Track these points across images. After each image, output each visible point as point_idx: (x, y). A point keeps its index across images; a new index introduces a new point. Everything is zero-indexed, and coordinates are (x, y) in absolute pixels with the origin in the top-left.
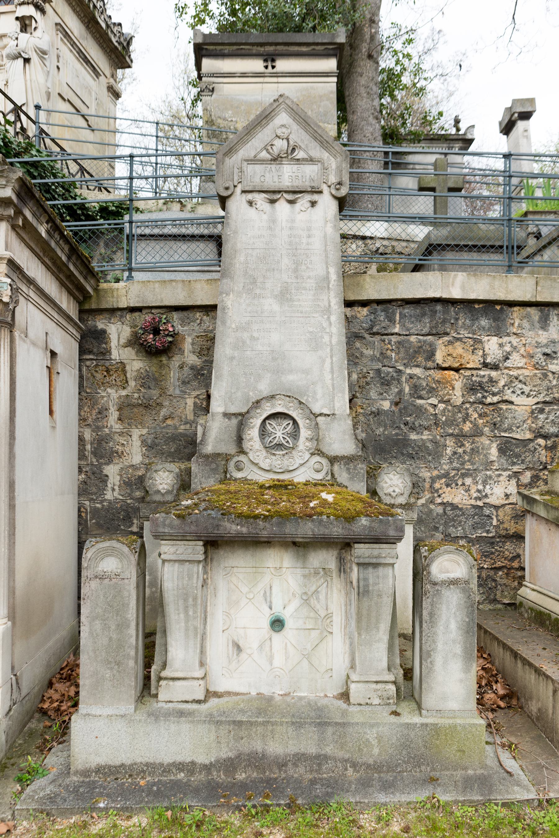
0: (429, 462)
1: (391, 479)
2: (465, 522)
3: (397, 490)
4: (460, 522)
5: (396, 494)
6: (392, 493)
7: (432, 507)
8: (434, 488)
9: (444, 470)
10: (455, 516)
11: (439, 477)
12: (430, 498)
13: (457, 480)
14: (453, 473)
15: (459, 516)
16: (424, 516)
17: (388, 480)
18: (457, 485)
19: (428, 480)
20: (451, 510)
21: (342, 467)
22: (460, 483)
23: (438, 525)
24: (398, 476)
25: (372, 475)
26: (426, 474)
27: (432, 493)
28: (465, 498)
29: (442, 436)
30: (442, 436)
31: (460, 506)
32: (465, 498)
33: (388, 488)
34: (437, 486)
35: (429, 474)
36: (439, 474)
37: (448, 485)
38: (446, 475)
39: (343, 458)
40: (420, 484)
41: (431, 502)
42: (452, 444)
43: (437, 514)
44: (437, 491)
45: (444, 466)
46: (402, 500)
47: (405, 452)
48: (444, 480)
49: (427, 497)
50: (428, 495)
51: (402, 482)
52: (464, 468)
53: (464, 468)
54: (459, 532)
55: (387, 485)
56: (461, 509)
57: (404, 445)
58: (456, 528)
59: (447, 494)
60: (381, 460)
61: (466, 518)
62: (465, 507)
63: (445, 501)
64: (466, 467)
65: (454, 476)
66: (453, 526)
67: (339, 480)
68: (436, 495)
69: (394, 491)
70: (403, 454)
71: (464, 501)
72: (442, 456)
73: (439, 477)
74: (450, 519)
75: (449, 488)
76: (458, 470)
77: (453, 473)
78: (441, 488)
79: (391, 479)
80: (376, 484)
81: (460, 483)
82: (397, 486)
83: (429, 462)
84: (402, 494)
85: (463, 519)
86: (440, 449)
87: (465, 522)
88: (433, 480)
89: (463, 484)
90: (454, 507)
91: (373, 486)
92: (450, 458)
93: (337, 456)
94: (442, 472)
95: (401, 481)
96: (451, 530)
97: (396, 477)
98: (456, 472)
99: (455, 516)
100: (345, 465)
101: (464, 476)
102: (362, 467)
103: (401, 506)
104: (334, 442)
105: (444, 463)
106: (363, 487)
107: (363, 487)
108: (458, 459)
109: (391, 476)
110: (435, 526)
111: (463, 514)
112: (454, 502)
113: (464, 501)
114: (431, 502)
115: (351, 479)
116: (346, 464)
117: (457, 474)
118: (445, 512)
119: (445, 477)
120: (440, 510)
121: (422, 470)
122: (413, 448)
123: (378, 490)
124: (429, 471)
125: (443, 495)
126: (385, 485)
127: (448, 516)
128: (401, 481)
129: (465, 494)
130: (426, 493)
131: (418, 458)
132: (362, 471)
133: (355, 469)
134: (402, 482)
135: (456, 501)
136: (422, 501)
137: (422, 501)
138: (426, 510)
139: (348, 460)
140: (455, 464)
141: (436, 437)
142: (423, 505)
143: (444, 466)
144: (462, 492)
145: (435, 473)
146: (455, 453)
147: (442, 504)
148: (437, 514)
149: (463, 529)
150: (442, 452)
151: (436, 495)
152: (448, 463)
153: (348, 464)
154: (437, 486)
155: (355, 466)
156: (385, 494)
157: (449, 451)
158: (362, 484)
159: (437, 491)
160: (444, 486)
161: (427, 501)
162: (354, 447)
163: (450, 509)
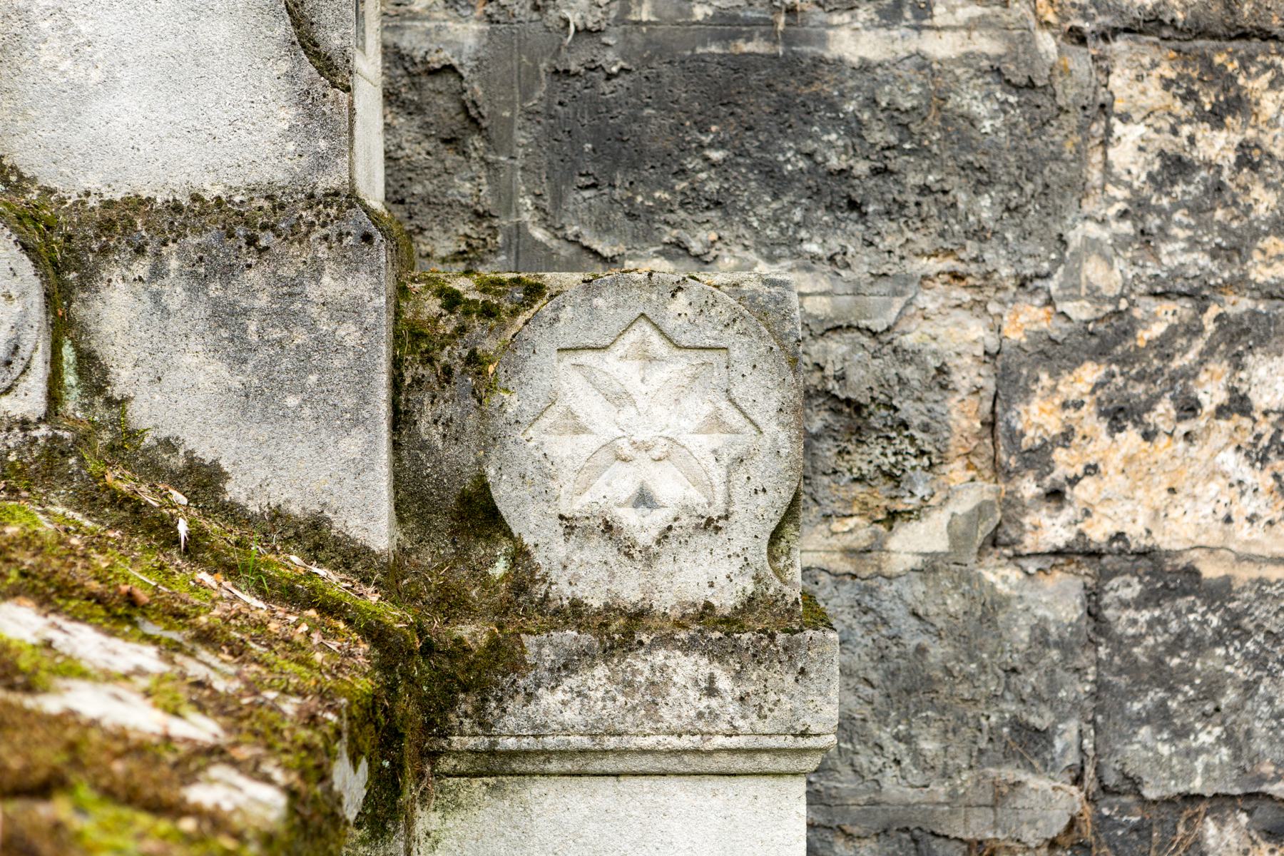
0: (979, 234)
1: (619, 398)
2: (1249, 688)
3: (673, 489)
4: (1212, 689)
5: (658, 519)
6: (629, 518)
7: (1000, 576)
8: (1014, 436)
9: (1094, 294)
10: (1175, 646)
11: (1054, 354)
12: (980, 511)
13: (1189, 374)
14: (1159, 319)
15: (1199, 647)
16: (938, 651)
17: (590, 406)
18: (1189, 408)
19: (967, 375)
20: (1140, 604)
21: (176, 295)
22: (1211, 392)
23: (1041, 719)
24: (678, 367)
25: (442, 365)
26: (952, 331)
27: (1000, 471)
28: (1248, 505)
29: (1078, 37)
30: (1078, 37)
31: (1211, 571)
32: (1248, 505)
33: (590, 470)
34: (1037, 417)
35: (976, 331)
36: (1056, 328)
37: (1118, 415)
38: (1108, 338)
39: (184, 214)
40: (908, 409)
41: (994, 541)
42: (1154, 95)
43: (1041, 636)
44: (1037, 459)
45: (1094, 271)
46: (709, 575)
47: (792, 163)
48: (1090, 373)
49: (965, 503)
50: (965, 491)
51: (716, 422)
52: (1240, 284)
53: (1240, 284)
54: (1205, 763)
55: (588, 443)
56: (1218, 593)
57: (784, 105)
58: (1182, 733)
59: (1113, 482)
60: (604, 228)
61: (1257, 660)
62: (1245, 574)
63: (1098, 533)
64: (1261, 274)
65: (1164, 347)
66: (1160, 717)
67: (151, 413)
68: (1028, 488)
69: (644, 499)
70: (775, 180)
71: (1242, 531)
72: (1080, 188)
73: (1054, 354)
74: (1131, 667)
75: (1130, 437)
76: (1198, 296)
77: (1159, 319)
78: (1066, 436)
79: (619, 398)
80: (490, 441)
81: (1211, 392)
82: (670, 452)
83: (979, 234)
84: (710, 525)
85: (1228, 662)
86: (1062, 135)
87: (1249, 688)
88: (1009, 374)
89: (1238, 404)
90: (1168, 577)
91: (463, 455)
92: (1136, 208)
93: (138, 204)
94: (1080, 311)
95: (699, 407)
96: (1144, 749)
97: (659, 375)
98: (1184, 308)
99: (1175, 646)
100: (198, 281)
101: (1239, 339)
102: (350, 300)
103: (710, 628)
104: (109, 82)
105: (1092, 245)
106: (361, 468)
107: (361, 468)
108: (1196, 209)
109: (617, 366)
110: (1018, 726)
111: (1234, 628)
112: (1164, 541)
113: (1242, 531)
114: (994, 541)
115: (257, 401)
116: (204, 270)
117: (1193, 331)
118: (1094, 613)
119: (1101, 352)
120: (1059, 600)
121: (926, 300)
122: (855, 130)
123: (505, 495)
124: (978, 307)
125: (1085, 491)
126: (563, 448)
127: (1118, 643)
128: (699, 407)
129: (1251, 476)
130: (956, 472)
131: (894, 210)
132: (349, 333)
133: (286, 317)
134: (716, 422)
135: (1181, 530)
136: (921, 538)
137: (921, 538)
138: (955, 603)
139: (232, 233)
140: (1175, 255)
141: (1027, 40)
142: (930, 566)
143: (1094, 271)
144: (1231, 461)
145: (1025, 320)
146: (1176, 167)
147: (1077, 553)
148: (1041, 636)
149: (1228, 739)
150: (1080, 156)
151: (1028, 488)
152: (1121, 243)
153: (227, 273)
154: (1037, 417)
155: (290, 291)
156: (569, 525)
157: (1130, 151)
158: (352, 445)
159: (1037, 459)
160: (1090, 421)
161: (957, 538)
162: (287, 116)
163: (1133, 590)
